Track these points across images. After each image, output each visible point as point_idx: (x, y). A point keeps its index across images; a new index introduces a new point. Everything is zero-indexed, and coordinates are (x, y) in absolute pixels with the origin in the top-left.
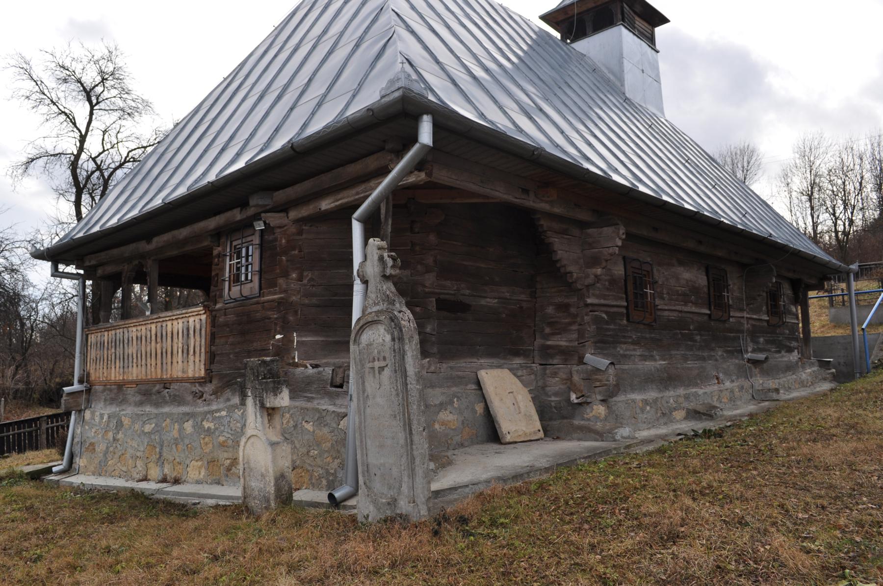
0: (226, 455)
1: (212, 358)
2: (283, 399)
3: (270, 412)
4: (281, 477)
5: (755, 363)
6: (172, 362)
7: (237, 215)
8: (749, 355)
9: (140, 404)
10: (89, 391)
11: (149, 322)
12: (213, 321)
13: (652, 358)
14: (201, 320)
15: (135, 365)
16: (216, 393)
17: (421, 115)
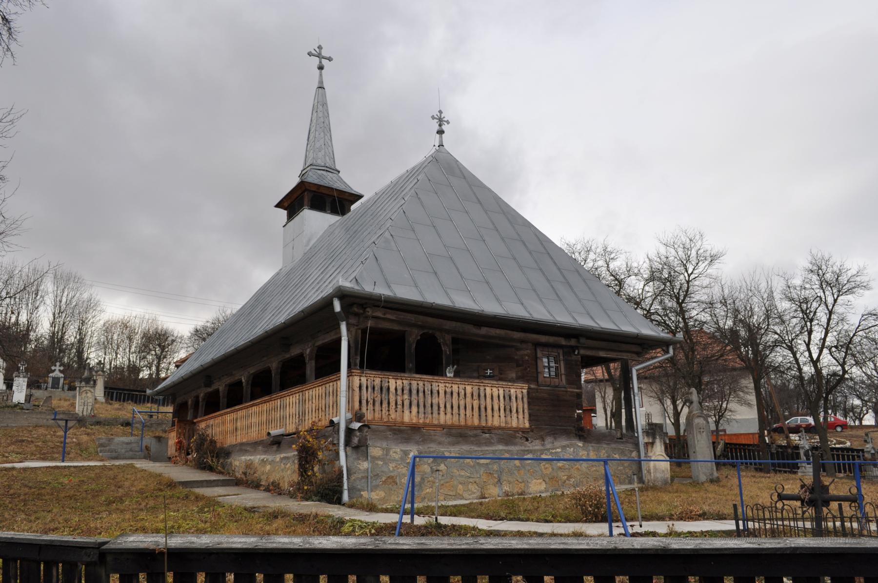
0: (563, 474)
6: (493, 416)
7: (563, 341)
9: (458, 443)
11: (467, 383)
14: (522, 392)
15: (442, 413)
17: (670, 345)
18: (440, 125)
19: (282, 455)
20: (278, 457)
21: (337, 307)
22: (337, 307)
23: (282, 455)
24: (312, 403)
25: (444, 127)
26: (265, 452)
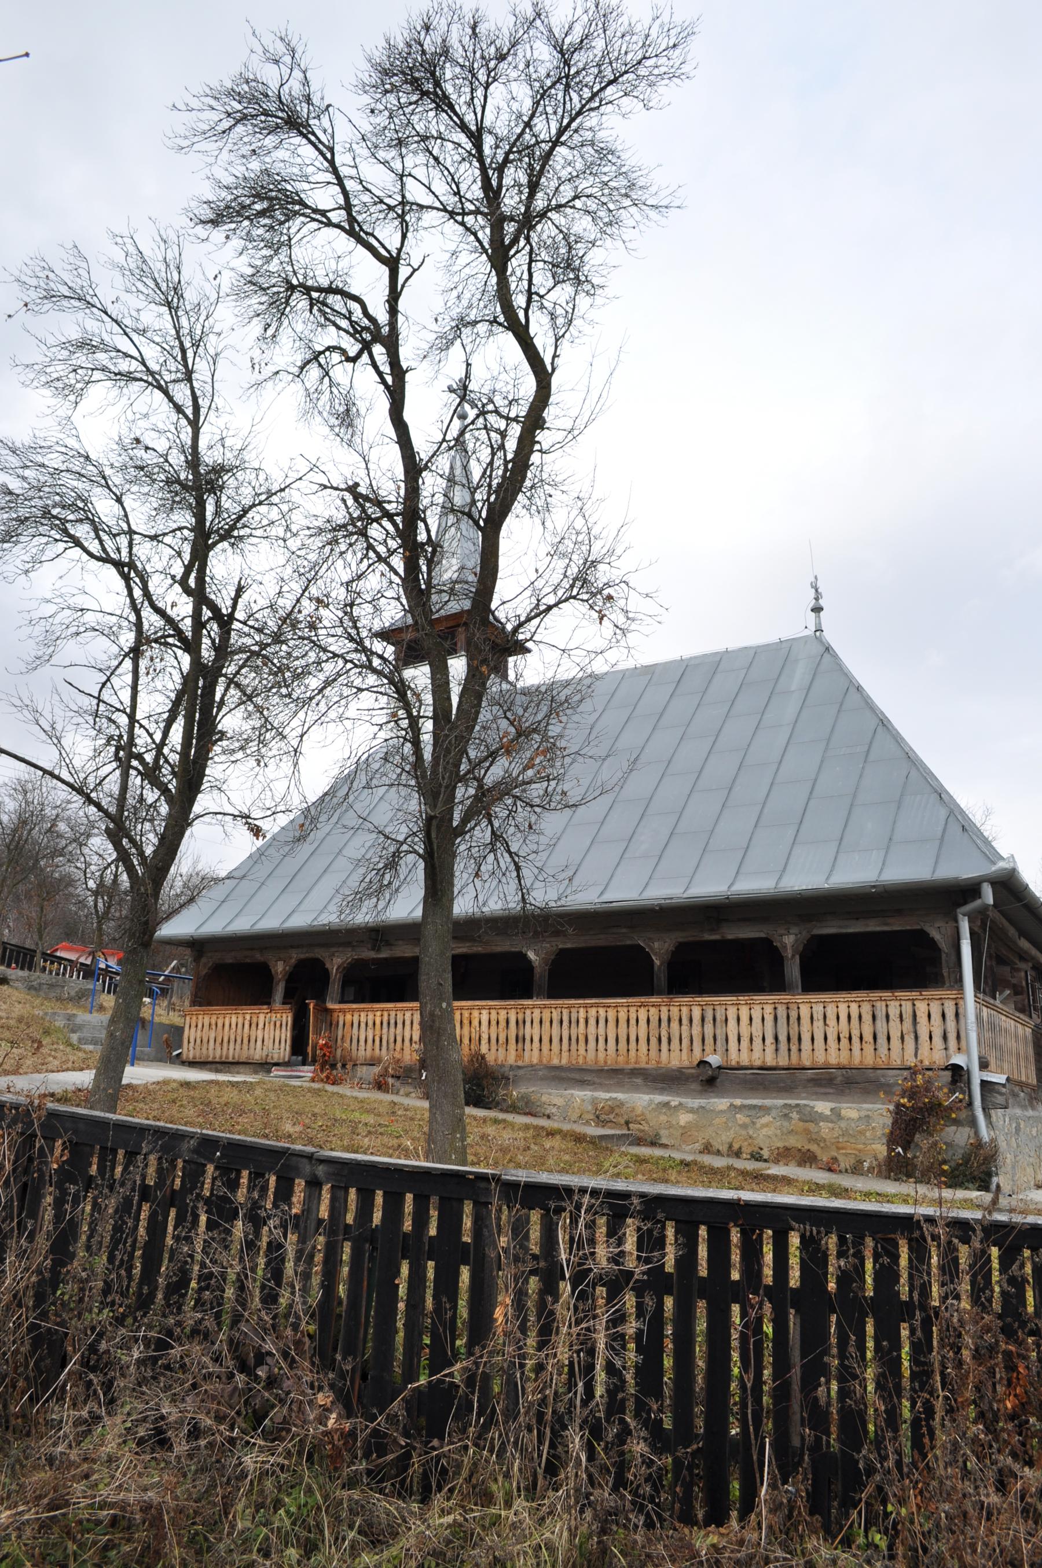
18: (817, 599)
19: (738, 1102)
20: (721, 1103)
21: (988, 895)
22: (988, 895)
23: (738, 1102)
24: (825, 1024)
25: (822, 602)
26: (662, 1091)
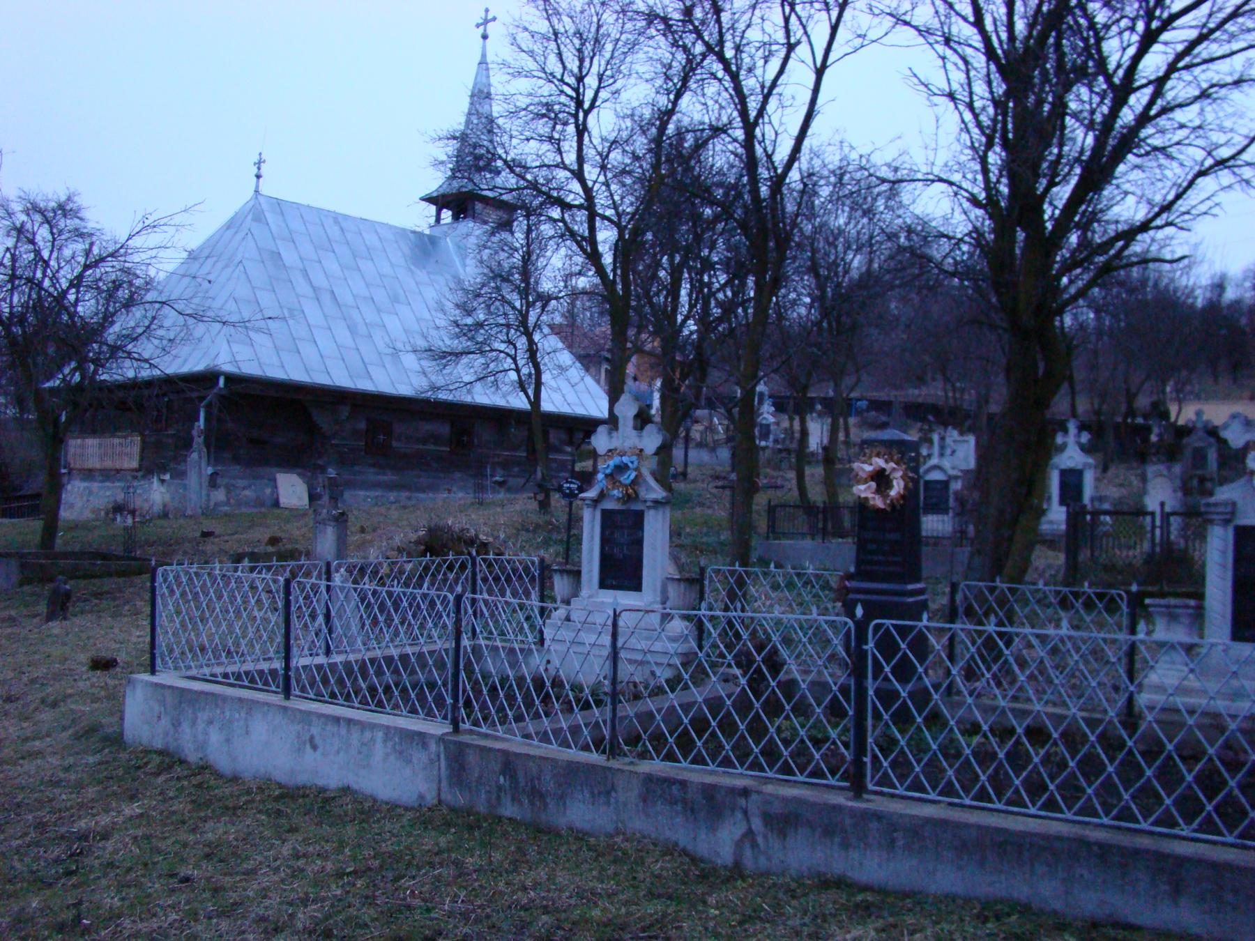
1: (142, 459)
2: (167, 477)
3: (163, 481)
4: (165, 506)
5: (501, 484)
8: (497, 478)
10: (69, 473)
12: (143, 441)
13: (384, 474)
16: (144, 477)
